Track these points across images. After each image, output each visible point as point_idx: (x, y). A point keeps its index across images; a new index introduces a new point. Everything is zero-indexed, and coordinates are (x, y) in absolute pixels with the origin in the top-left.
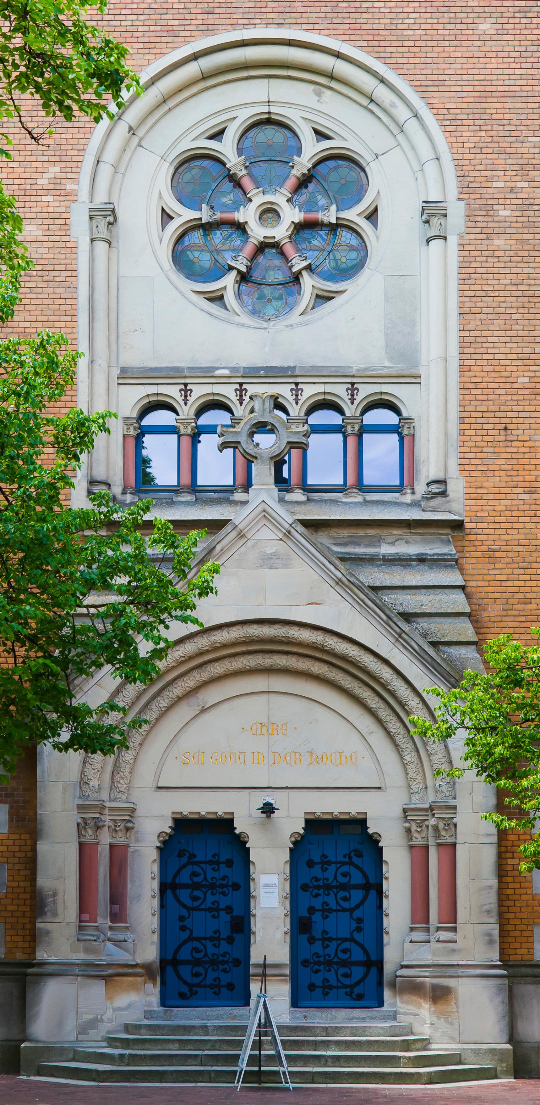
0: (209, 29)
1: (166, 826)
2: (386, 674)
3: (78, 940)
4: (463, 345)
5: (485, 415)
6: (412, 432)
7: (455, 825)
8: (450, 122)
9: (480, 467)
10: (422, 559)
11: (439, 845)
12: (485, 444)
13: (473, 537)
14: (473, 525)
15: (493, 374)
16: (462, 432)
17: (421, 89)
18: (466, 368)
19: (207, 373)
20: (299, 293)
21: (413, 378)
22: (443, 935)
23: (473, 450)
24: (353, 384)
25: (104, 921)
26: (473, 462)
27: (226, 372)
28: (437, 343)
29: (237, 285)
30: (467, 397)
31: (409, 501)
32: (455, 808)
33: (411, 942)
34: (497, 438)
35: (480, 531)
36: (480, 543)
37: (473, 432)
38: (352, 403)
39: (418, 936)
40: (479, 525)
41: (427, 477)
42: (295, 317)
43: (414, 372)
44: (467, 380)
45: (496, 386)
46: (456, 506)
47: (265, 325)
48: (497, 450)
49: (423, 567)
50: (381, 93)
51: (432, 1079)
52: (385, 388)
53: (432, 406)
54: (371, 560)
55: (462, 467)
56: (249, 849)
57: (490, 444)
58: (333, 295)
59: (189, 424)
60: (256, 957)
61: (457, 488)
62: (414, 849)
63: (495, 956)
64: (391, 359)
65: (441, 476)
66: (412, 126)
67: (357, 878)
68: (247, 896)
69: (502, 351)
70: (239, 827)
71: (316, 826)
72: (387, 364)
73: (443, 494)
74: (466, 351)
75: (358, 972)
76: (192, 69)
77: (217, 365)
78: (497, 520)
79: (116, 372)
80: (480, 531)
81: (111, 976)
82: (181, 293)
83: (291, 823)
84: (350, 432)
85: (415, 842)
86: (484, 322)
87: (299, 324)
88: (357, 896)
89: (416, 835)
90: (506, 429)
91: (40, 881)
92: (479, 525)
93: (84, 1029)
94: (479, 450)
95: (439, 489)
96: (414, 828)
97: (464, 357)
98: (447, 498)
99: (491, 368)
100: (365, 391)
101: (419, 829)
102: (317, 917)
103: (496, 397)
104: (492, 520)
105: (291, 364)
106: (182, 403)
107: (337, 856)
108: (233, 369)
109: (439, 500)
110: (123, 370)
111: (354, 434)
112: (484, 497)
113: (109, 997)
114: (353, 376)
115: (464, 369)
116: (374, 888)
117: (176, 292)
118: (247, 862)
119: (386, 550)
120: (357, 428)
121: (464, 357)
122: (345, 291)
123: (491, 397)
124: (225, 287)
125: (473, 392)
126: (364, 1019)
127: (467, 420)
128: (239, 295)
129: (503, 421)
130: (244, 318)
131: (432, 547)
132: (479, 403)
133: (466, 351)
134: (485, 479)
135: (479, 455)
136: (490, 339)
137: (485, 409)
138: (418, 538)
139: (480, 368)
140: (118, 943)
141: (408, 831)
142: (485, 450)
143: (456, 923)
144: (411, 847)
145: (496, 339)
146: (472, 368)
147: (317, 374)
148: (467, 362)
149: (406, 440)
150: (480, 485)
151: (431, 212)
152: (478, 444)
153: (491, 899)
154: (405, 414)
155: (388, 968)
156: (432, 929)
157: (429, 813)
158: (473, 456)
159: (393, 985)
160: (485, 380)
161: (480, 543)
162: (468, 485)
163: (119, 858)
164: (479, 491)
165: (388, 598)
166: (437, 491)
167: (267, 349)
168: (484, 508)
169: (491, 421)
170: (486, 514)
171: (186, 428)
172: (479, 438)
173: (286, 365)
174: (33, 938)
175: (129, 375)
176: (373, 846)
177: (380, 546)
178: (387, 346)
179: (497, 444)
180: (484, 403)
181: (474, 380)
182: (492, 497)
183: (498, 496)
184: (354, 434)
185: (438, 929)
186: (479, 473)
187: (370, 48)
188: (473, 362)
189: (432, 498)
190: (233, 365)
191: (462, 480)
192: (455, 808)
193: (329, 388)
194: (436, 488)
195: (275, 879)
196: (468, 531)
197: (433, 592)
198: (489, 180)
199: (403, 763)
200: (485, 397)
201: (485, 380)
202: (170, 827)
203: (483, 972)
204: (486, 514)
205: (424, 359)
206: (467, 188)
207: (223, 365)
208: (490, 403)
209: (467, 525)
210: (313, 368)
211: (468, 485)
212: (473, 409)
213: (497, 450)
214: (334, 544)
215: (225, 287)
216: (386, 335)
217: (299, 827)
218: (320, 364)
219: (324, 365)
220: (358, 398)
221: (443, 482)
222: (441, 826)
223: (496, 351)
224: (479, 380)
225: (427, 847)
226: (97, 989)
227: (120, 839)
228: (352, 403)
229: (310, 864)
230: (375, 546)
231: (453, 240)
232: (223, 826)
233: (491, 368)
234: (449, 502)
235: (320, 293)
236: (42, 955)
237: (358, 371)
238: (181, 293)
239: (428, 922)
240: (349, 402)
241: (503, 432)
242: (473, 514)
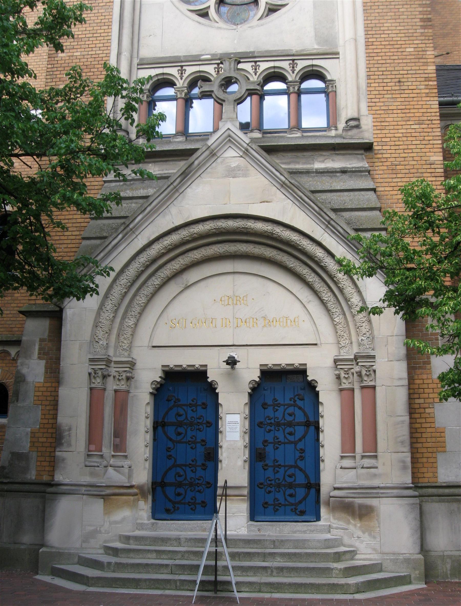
1: (157, 376)
2: (319, 253)
3: (86, 466)
4: (367, 29)
5: (384, 73)
6: (334, 90)
7: (375, 371)
9: (383, 108)
10: (344, 171)
11: (362, 388)
12: (385, 92)
13: (380, 156)
14: (380, 148)
15: (389, 47)
16: (369, 85)
18: (370, 44)
19: (196, 59)
20: (258, 9)
21: (334, 55)
22: (367, 462)
23: (377, 96)
24: (293, 60)
25: (107, 451)
26: (378, 104)
27: (209, 57)
29: (217, 6)
30: (371, 62)
31: (333, 135)
32: (374, 357)
33: (341, 468)
34: (393, 88)
35: (385, 152)
36: (385, 160)
37: (377, 85)
38: (293, 72)
39: (347, 463)
40: (384, 148)
41: (347, 114)
42: (254, 22)
43: (334, 50)
44: (371, 51)
45: (392, 54)
46: (367, 133)
47: (235, 27)
48: (394, 96)
49: (345, 176)
51: (359, 589)
52: (315, 62)
53: (348, 72)
54: (308, 172)
55: (370, 108)
56: (217, 394)
57: (389, 92)
58: (279, 8)
59: (183, 91)
61: (367, 123)
62: (343, 392)
63: (408, 479)
64: (318, 44)
65: (355, 115)
67: (300, 417)
68: (216, 432)
69: (394, 32)
70: (211, 376)
71: (269, 375)
72: (316, 47)
73: (358, 127)
74: (369, 33)
75: (301, 492)
77: (203, 53)
78: (397, 143)
79: (136, 61)
80: (385, 152)
81: (110, 495)
82: (180, 11)
83: (250, 373)
84: (292, 91)
85: (344, 386)
86: (380, 14)
87: (258, 26)
88: (300, 431)
89: (344, 381)
90: (399, 82)
91: (61, 419)
92: (384, 148)
93: (87, 538)
94: (382, 96)
95: (354, 123)
96: (343, 375)
97: (368, 36)
98: (361, 130)
99: (387, 43)
100: (301, 64)
101: (346, 376)
102: (270, 449)
103: (392, 61)
104: (393, 143)
105: (252, 50)
106: (179, 78)
107: (284, 394)
108: (212, 55)
109: (355, 131)
110: (142, 59)
111: (295, 92)
112: (387, 128)
113: (107, 512)
114: (293, 55)
115: (368, 44)
116: (313, 426)
117: (177, 11)
118: (217, 405)
119: (318, 165)
120: (296, 88)
121: (368, 36)
122: (287, 5)
123: (388, 61)
124: (209, 6)
125: (375, 58)
126: (305, 532)
127: (372, 77)
128: (218, 11)
129: (397, 76)
130: (221, 24)
131: (351, 163)
132: (380, 65)
133: (369, 33)
134: (387, 116)
135: (381, 100)
136: (385, 25)
137: (385, 69)
138: (340, 157)
139: (379, 43)
140: (117, 468)
141: (338, 377)
142: (385, 96)
143: (376, 452)
144: (341, 390)
145: (389, 25)
146: (374, 43)
148: (370, 40)
149: (330, 95)
150: (383, 120)
152: (381, 92)
153: (405, 431)
154: (329, 78)
155: (324, 490)
156: (358, 457)
157: (354, 363)
158: (378, 100)
159: (328, 504)
160: (383, 50)
161: (385, 160)
162: (375, 120)
164: (383, 124)
166: (353, 125)
167: (236, 42)
168: (387, 135)
169: (389, 77)
170: (389, 140)
171: (181, 94)
172: (382, 88)
173: (248, 51)
174: (53, 463)
175: (145, 62)
176: (311, 387)
177: (313, 164)
178: (316, 35)
179: (394, 92)
180: (384, 65)
181: (375, 51)
182: (392, 127)
183: (396, 127)
184: (295, 92)
185: (363, 457)
186: (382, 112)
188: (374, 40)
189: (350, 130)
190: (213, 52)
191: (371, 117)
192: (374, 357)
193: (277, 64)
194: (352, 123)
195: (237, 418)
196: (376, 152)
199: (334, 324)
200: (384, 62)
201: (383, 50)
202: (160, 377)
203: (399, 493)
204: (389, 140)
205: (341, 42)
207: (207, 53)
208: (388, 65)
209: (376, 148)
210: (266, 51)
211: (375, 120)
212: (376, 69)
213: (394, 96)
214: (281, 163)
215: (209, 6)
216: (315, 29)
217: (255, 376)
218: (271, 49)
219: (274, 49)
220: (297, 69)
221: (357, 119)
222: (364, 372)
223: (390, 32)
224: (379, 51)
225: (353, 390)
226: (98, 505)
227: (123, 386)
228: (293, 72)
229: (265, 406)
230: (310, 164)
232: (198, 376)
233: (387, 43)
234: (362, 132)
235: (271, 7)
236: (59, 477)
237: (297, 51)
238: (180, 11)
239: (354, 451)
240: (291, 72)
241: (397, 84)
242: (379, 140)
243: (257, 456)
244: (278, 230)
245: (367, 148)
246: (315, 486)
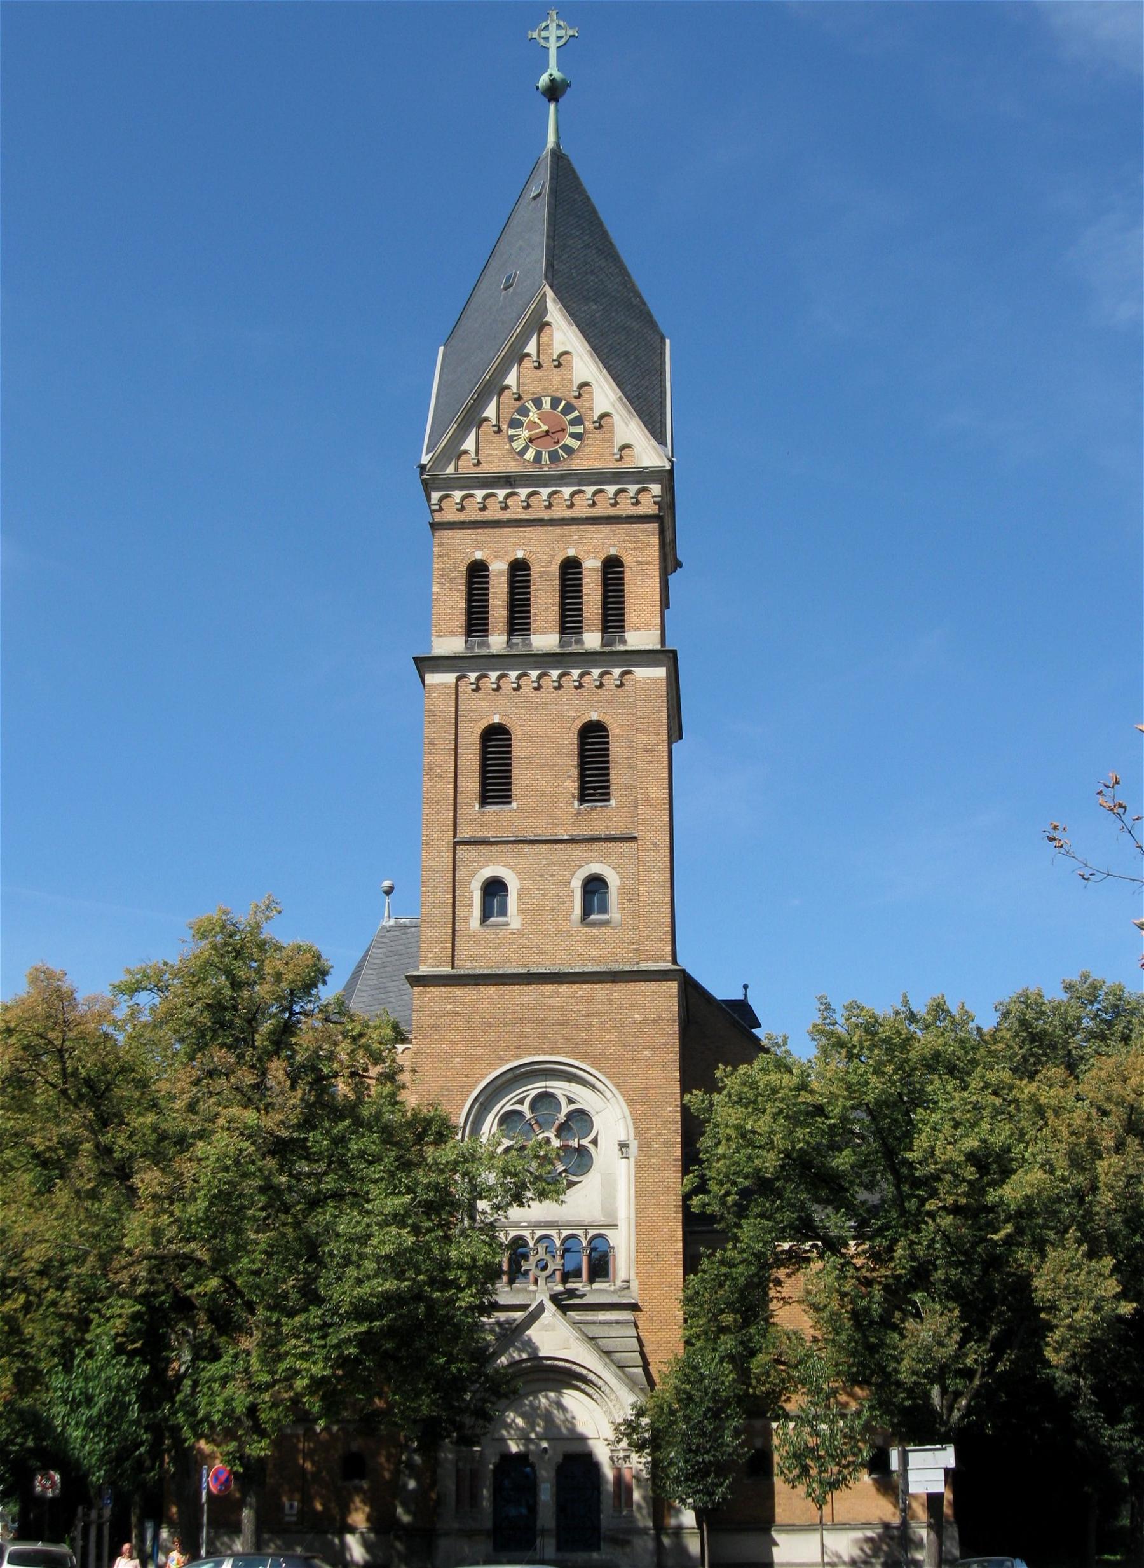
0: (518, 1057)
8: (630, 1101)
10: (617, 1322)
16: (637, 1257)
17: (617, 1085)
28: (625, 1209)
49: (619, 1326)
50: (598, 1084)
60: (539, 1525)
61: (635, 1285)
66: (613, 1100)
76: (509, 1075)
109: (626, 1292)
115: (637, 1225)
147: (569, 1225)
151: (623, 1146)
155: (603, 1530)
163: (475, 1476)
165: (601, 1342)
187: (592, 1065)
197: (623, 1340)
198: (648, 1129)
206: (639, 1133)
231: (632, 1159)
243: (562, 1508)
244: (574, 1367)
245: (634, 1307)
246: (596, 1528)
